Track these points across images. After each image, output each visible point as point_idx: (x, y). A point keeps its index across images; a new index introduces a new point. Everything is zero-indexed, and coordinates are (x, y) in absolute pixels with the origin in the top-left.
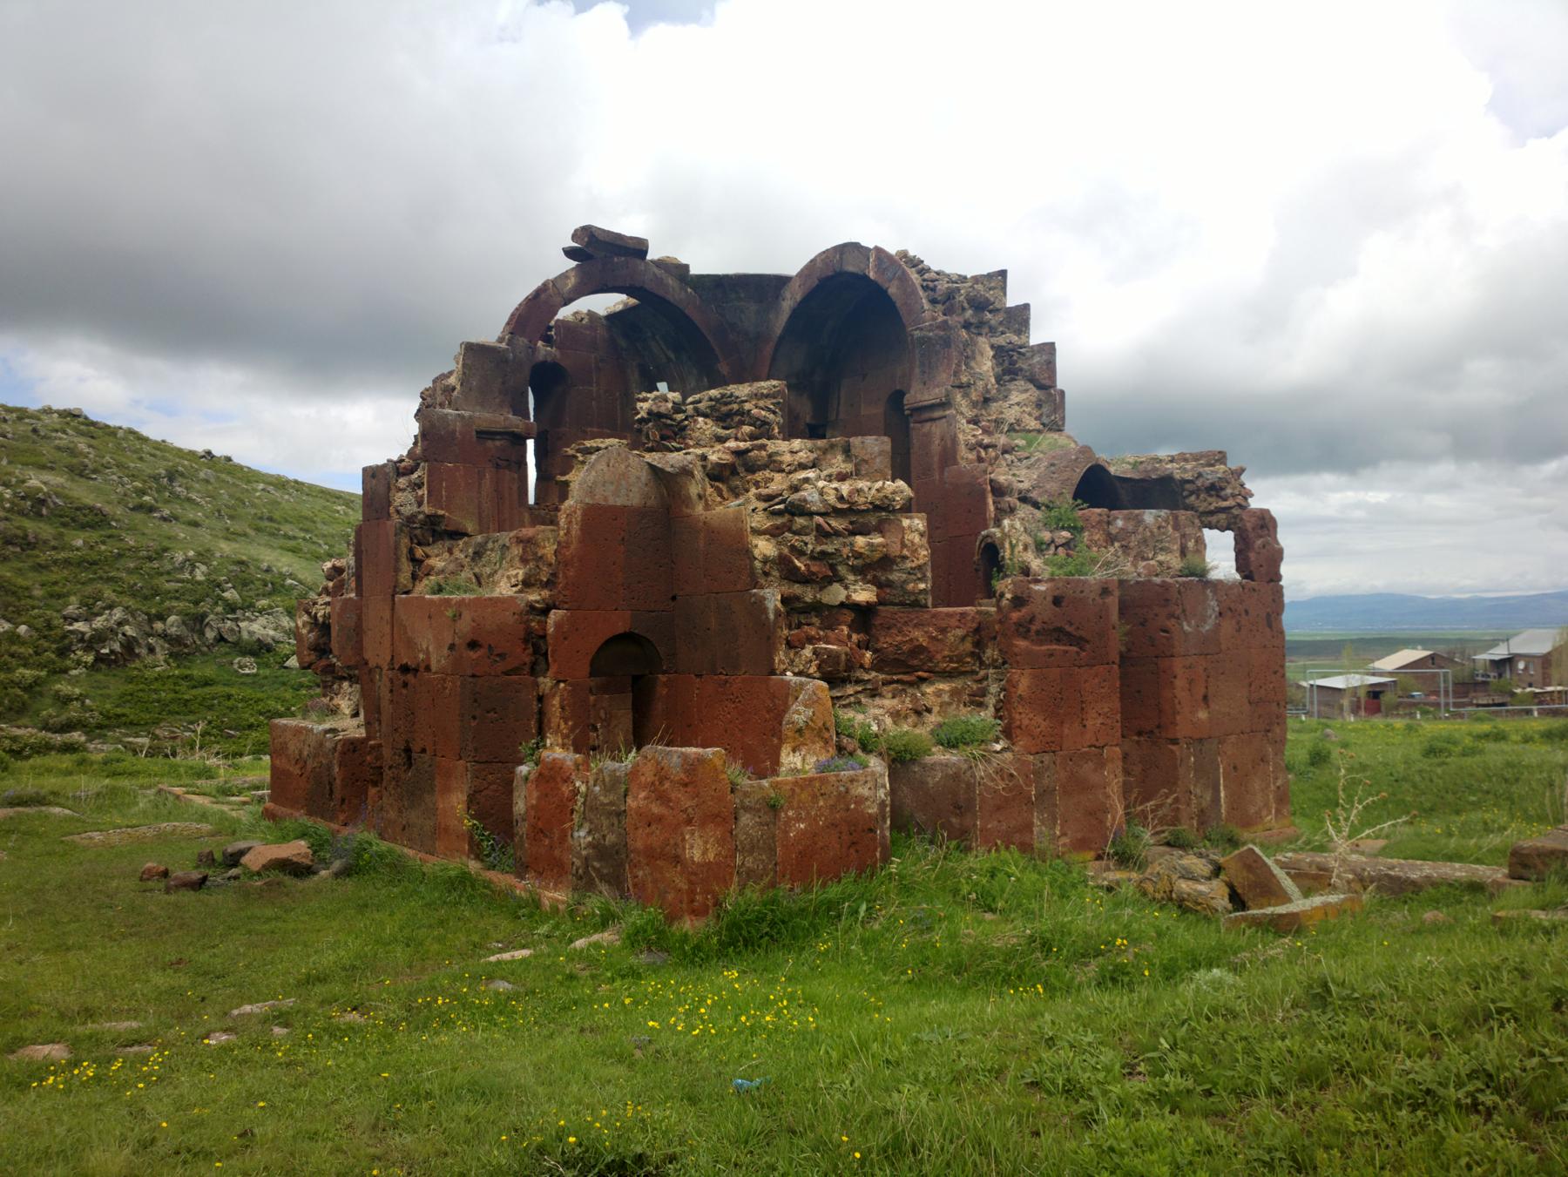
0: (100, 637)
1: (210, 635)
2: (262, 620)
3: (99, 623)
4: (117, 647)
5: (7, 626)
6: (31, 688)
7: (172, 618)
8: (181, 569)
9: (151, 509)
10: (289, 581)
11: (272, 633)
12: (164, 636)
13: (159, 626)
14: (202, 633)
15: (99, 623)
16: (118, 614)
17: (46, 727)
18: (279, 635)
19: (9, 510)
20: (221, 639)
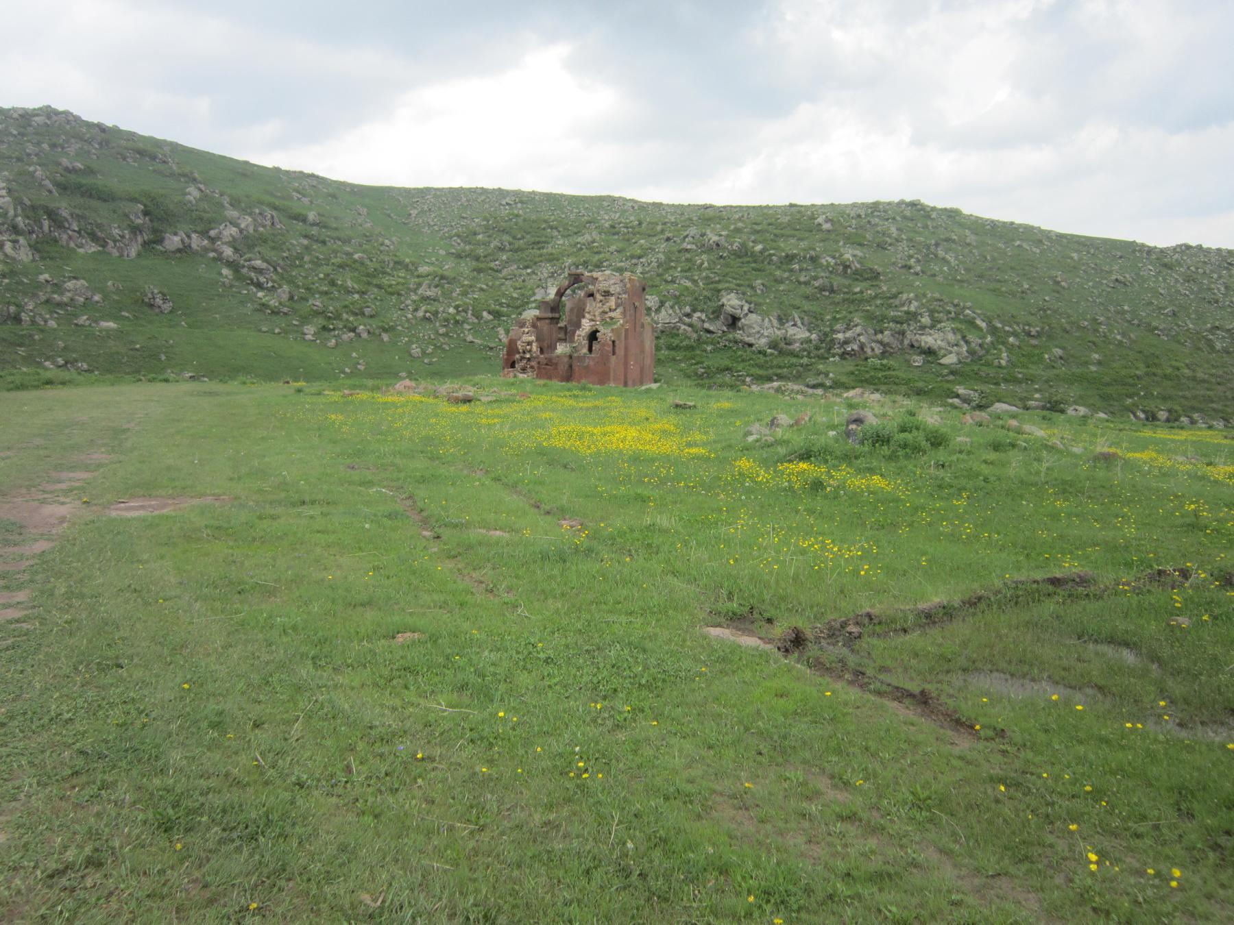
0: (846, 342)
1: (906, 342)
2: (936, 336)
3: (849, 334)
4: (855, 347)
5: (808, 334)
6: (807, 367)
7: (886, 333)
8: (903, 305)
9: (910, 268)
10: (968, 311)
11: (939, 342)
12: (881, 342)
13: (879, 336)
14: (902, 342)
15: (849, 334)
16: (858, 330)
17: (808, 386)
18: (943, 344)
19: (831, 272)
20: (912, 346)
